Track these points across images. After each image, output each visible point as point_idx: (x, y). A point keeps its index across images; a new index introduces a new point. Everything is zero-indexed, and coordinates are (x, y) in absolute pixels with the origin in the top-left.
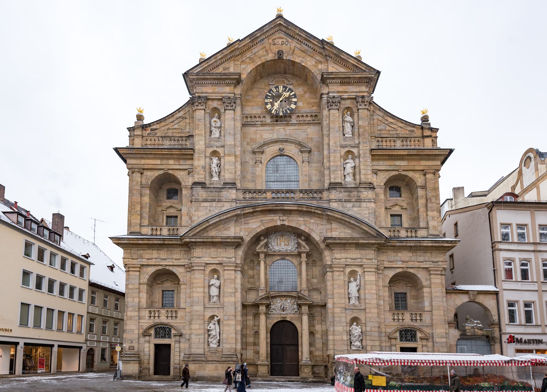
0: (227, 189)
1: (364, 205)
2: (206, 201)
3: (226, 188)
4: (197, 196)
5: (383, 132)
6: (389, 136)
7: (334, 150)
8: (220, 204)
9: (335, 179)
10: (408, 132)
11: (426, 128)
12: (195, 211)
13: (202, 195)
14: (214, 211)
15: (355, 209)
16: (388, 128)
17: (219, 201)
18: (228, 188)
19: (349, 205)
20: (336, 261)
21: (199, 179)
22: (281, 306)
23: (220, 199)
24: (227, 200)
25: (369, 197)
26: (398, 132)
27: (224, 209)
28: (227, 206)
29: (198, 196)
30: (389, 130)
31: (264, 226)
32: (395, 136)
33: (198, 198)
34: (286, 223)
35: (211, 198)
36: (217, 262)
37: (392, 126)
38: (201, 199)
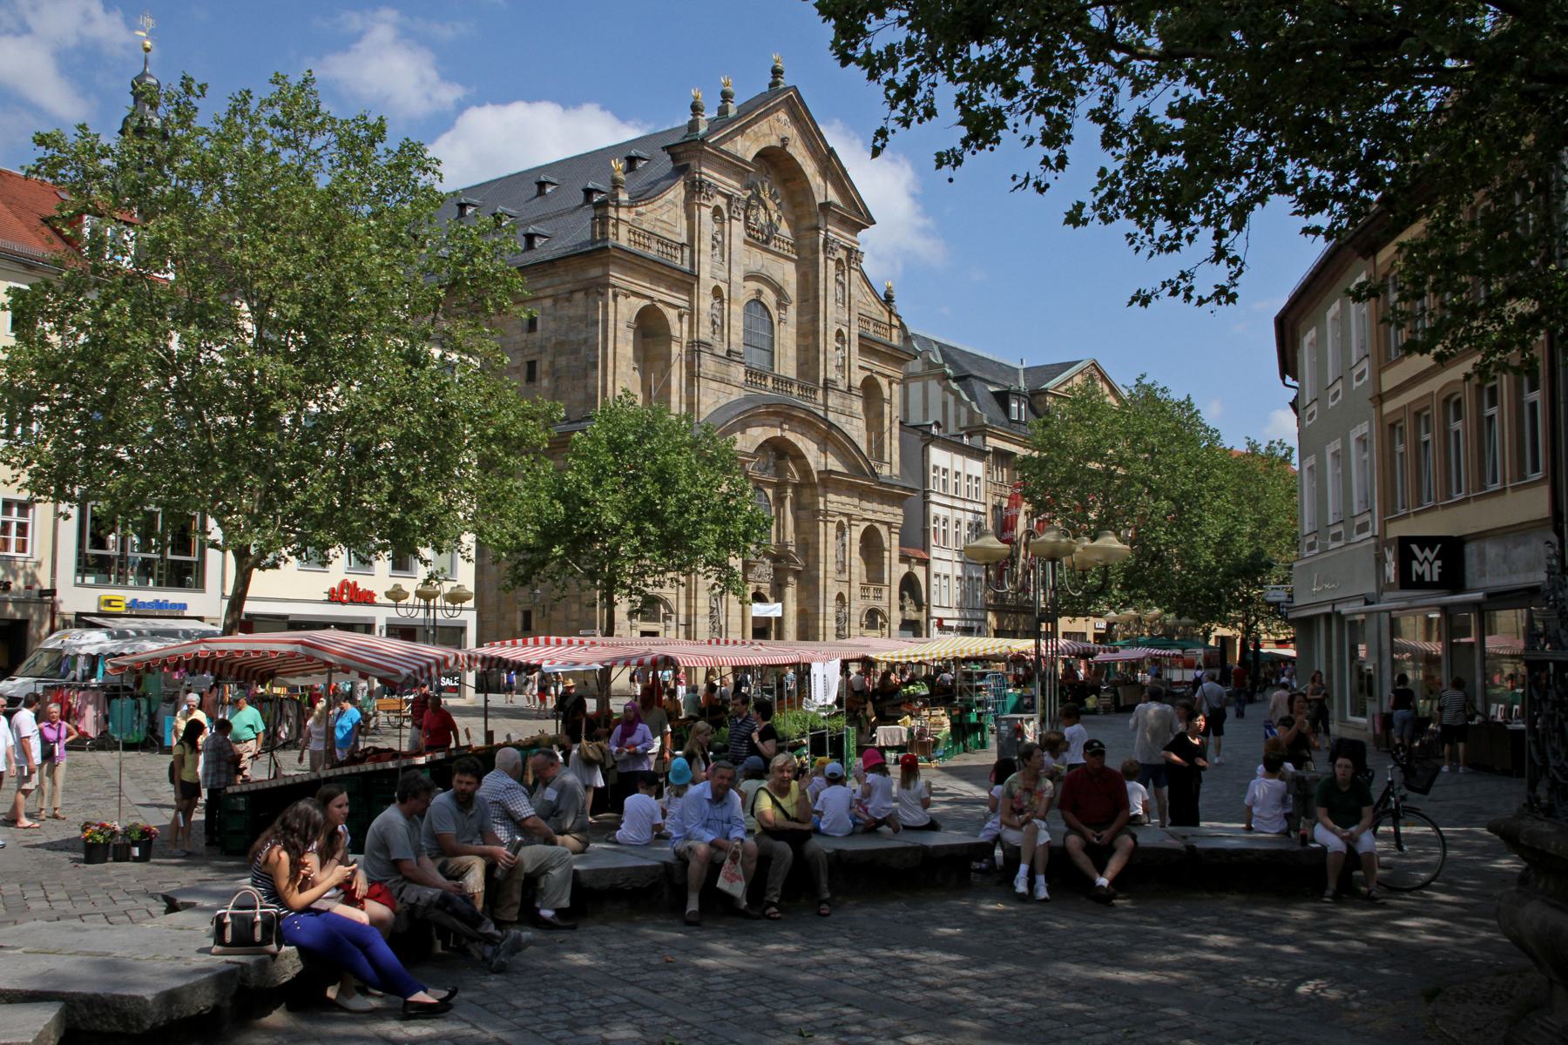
15: (848, 427)
19: (843, 419)
27: (733, 398)
28: (737, 394)
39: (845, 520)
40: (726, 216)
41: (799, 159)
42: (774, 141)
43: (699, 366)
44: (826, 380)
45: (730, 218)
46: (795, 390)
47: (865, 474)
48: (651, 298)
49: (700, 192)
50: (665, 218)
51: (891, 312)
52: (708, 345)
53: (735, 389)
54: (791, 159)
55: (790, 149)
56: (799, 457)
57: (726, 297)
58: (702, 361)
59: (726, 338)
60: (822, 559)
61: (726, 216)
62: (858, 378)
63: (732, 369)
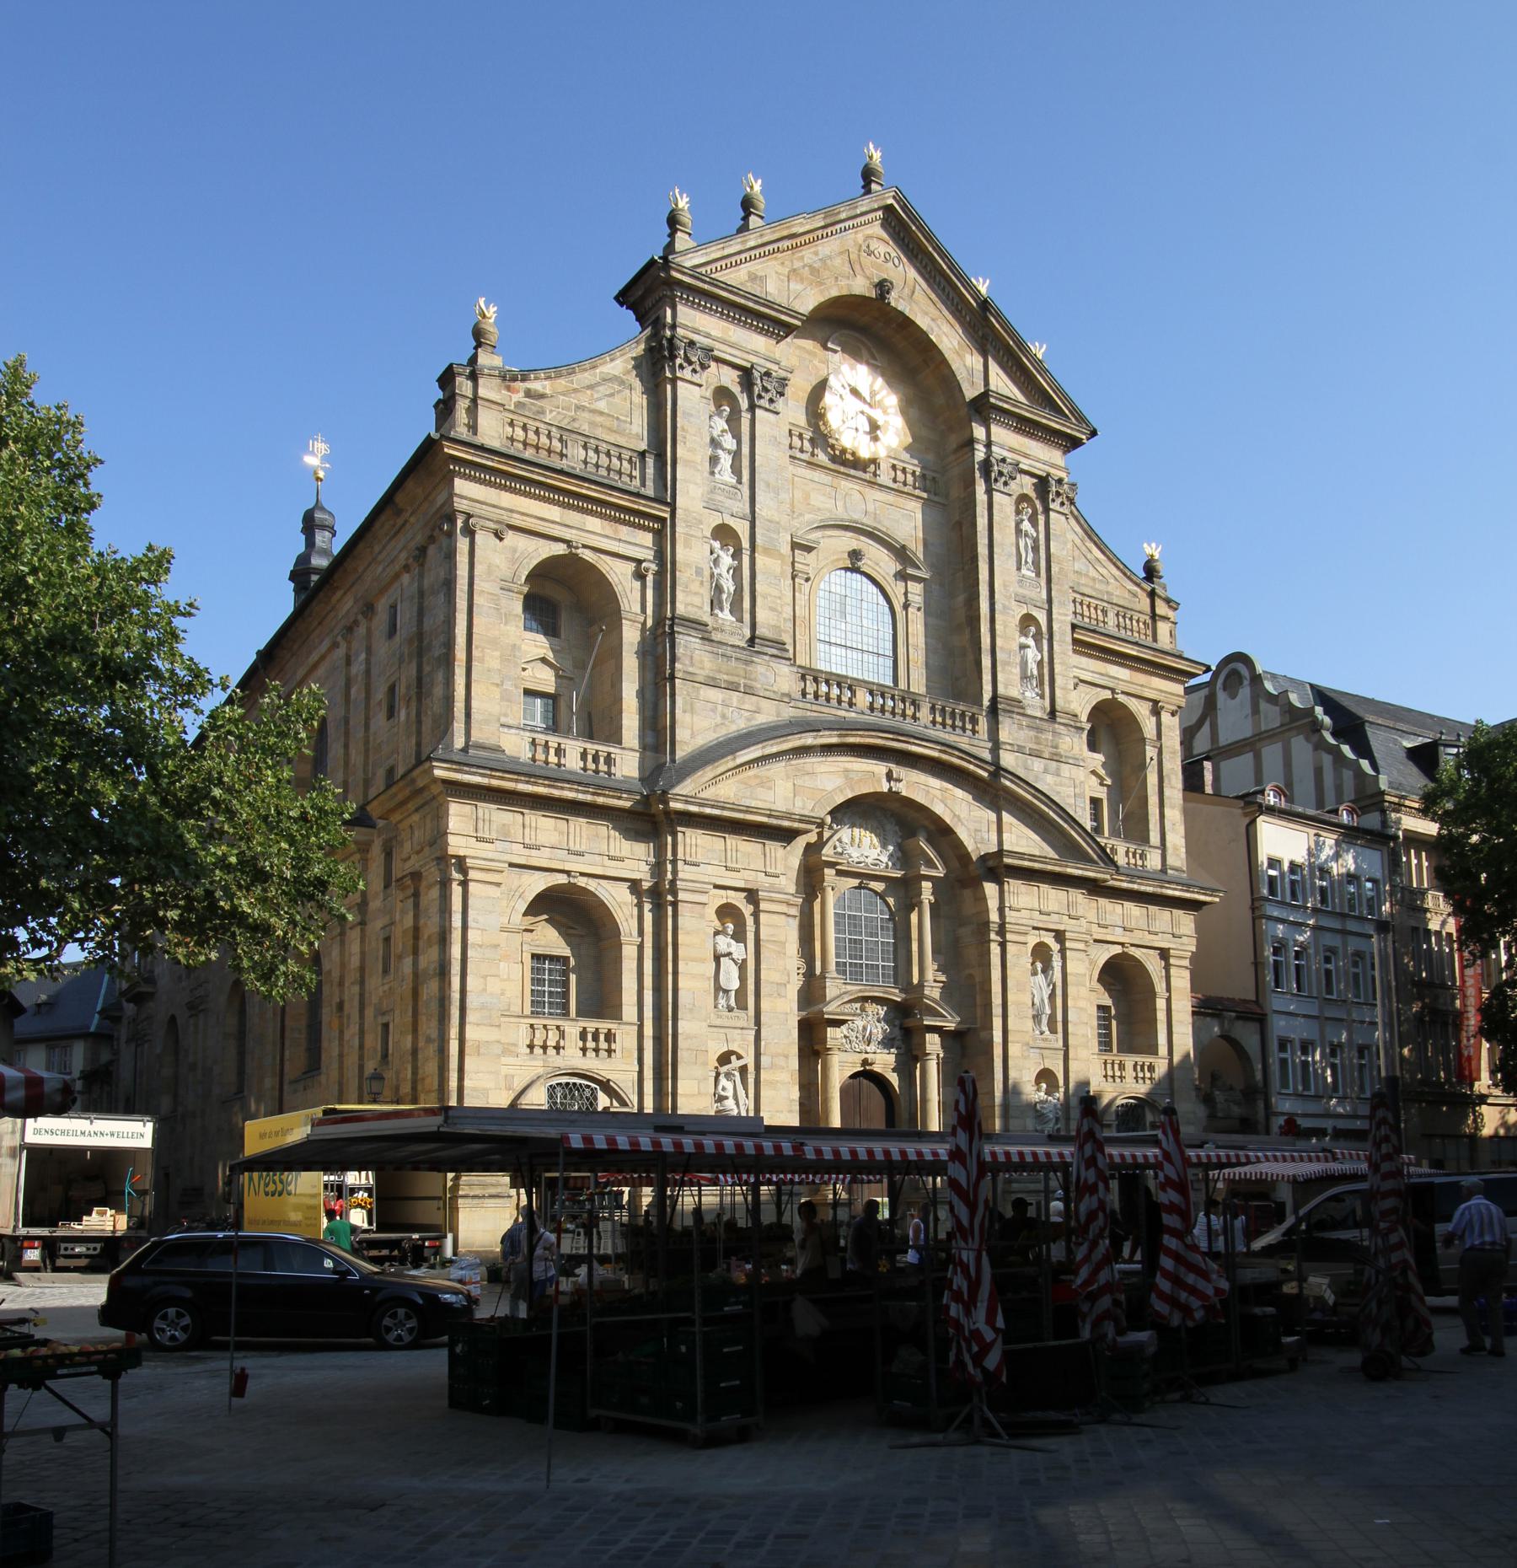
0: (767, 658)
1: (1066, 770)
2: (712, 683)
3: (766, 654)
4: (687, 662)
5: (1083, 581)
6: (1094, 594)
7: (1004, 607)
8: (750, 702)
9: (1006, 687)
10: (1127, 595)
11: (1160, 597)
12: (684, 711)
13: (702, 662)
14: (733, 722)
15: (1049, 779)
16: (1092, 573)
17: (749, 692)
18: (772, 656)
19: (1037, 765)
20: (1013, 913)
21: (690, 608)
22: (865, 1028)
23: (751, 687)
24: (767, 694)
25: (1074, 752)
26: (1110, 589)
29: (692, 665)
30: (1094, 579)
31: (852, 790)
32: (1105, 598)
33: (691, 669)
34: (903, 789)
35: (725, 677)
36: (741, 885)
37: (1101, 570)
38: (701, 674)
39: (1049, 939)
40: (744, 403)
41: (922, 322)
42: (861, 286)
43: (673, 660)
44: (995, 698)
45: (752, 408)
46: (924, 714)
47: (1092, 861)
48: (568, 543)
49: (673, 357)
50: (602, 405)
51: (1152, 595)
52: (696, 625)
53: (765, 704)
54: (906, 323)
55: (896, 300)
56: (942, 833)
57: (746, 544)
58: (680, 651)
59: (747, 617)
60: (997, 1010)
61: (744, 403)
62: (1080, 703)
63: (761, 669)
